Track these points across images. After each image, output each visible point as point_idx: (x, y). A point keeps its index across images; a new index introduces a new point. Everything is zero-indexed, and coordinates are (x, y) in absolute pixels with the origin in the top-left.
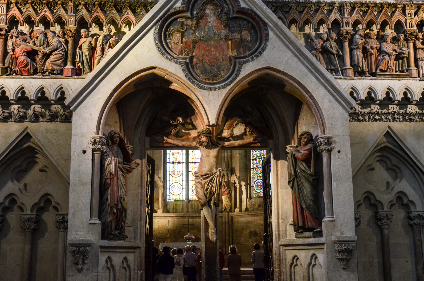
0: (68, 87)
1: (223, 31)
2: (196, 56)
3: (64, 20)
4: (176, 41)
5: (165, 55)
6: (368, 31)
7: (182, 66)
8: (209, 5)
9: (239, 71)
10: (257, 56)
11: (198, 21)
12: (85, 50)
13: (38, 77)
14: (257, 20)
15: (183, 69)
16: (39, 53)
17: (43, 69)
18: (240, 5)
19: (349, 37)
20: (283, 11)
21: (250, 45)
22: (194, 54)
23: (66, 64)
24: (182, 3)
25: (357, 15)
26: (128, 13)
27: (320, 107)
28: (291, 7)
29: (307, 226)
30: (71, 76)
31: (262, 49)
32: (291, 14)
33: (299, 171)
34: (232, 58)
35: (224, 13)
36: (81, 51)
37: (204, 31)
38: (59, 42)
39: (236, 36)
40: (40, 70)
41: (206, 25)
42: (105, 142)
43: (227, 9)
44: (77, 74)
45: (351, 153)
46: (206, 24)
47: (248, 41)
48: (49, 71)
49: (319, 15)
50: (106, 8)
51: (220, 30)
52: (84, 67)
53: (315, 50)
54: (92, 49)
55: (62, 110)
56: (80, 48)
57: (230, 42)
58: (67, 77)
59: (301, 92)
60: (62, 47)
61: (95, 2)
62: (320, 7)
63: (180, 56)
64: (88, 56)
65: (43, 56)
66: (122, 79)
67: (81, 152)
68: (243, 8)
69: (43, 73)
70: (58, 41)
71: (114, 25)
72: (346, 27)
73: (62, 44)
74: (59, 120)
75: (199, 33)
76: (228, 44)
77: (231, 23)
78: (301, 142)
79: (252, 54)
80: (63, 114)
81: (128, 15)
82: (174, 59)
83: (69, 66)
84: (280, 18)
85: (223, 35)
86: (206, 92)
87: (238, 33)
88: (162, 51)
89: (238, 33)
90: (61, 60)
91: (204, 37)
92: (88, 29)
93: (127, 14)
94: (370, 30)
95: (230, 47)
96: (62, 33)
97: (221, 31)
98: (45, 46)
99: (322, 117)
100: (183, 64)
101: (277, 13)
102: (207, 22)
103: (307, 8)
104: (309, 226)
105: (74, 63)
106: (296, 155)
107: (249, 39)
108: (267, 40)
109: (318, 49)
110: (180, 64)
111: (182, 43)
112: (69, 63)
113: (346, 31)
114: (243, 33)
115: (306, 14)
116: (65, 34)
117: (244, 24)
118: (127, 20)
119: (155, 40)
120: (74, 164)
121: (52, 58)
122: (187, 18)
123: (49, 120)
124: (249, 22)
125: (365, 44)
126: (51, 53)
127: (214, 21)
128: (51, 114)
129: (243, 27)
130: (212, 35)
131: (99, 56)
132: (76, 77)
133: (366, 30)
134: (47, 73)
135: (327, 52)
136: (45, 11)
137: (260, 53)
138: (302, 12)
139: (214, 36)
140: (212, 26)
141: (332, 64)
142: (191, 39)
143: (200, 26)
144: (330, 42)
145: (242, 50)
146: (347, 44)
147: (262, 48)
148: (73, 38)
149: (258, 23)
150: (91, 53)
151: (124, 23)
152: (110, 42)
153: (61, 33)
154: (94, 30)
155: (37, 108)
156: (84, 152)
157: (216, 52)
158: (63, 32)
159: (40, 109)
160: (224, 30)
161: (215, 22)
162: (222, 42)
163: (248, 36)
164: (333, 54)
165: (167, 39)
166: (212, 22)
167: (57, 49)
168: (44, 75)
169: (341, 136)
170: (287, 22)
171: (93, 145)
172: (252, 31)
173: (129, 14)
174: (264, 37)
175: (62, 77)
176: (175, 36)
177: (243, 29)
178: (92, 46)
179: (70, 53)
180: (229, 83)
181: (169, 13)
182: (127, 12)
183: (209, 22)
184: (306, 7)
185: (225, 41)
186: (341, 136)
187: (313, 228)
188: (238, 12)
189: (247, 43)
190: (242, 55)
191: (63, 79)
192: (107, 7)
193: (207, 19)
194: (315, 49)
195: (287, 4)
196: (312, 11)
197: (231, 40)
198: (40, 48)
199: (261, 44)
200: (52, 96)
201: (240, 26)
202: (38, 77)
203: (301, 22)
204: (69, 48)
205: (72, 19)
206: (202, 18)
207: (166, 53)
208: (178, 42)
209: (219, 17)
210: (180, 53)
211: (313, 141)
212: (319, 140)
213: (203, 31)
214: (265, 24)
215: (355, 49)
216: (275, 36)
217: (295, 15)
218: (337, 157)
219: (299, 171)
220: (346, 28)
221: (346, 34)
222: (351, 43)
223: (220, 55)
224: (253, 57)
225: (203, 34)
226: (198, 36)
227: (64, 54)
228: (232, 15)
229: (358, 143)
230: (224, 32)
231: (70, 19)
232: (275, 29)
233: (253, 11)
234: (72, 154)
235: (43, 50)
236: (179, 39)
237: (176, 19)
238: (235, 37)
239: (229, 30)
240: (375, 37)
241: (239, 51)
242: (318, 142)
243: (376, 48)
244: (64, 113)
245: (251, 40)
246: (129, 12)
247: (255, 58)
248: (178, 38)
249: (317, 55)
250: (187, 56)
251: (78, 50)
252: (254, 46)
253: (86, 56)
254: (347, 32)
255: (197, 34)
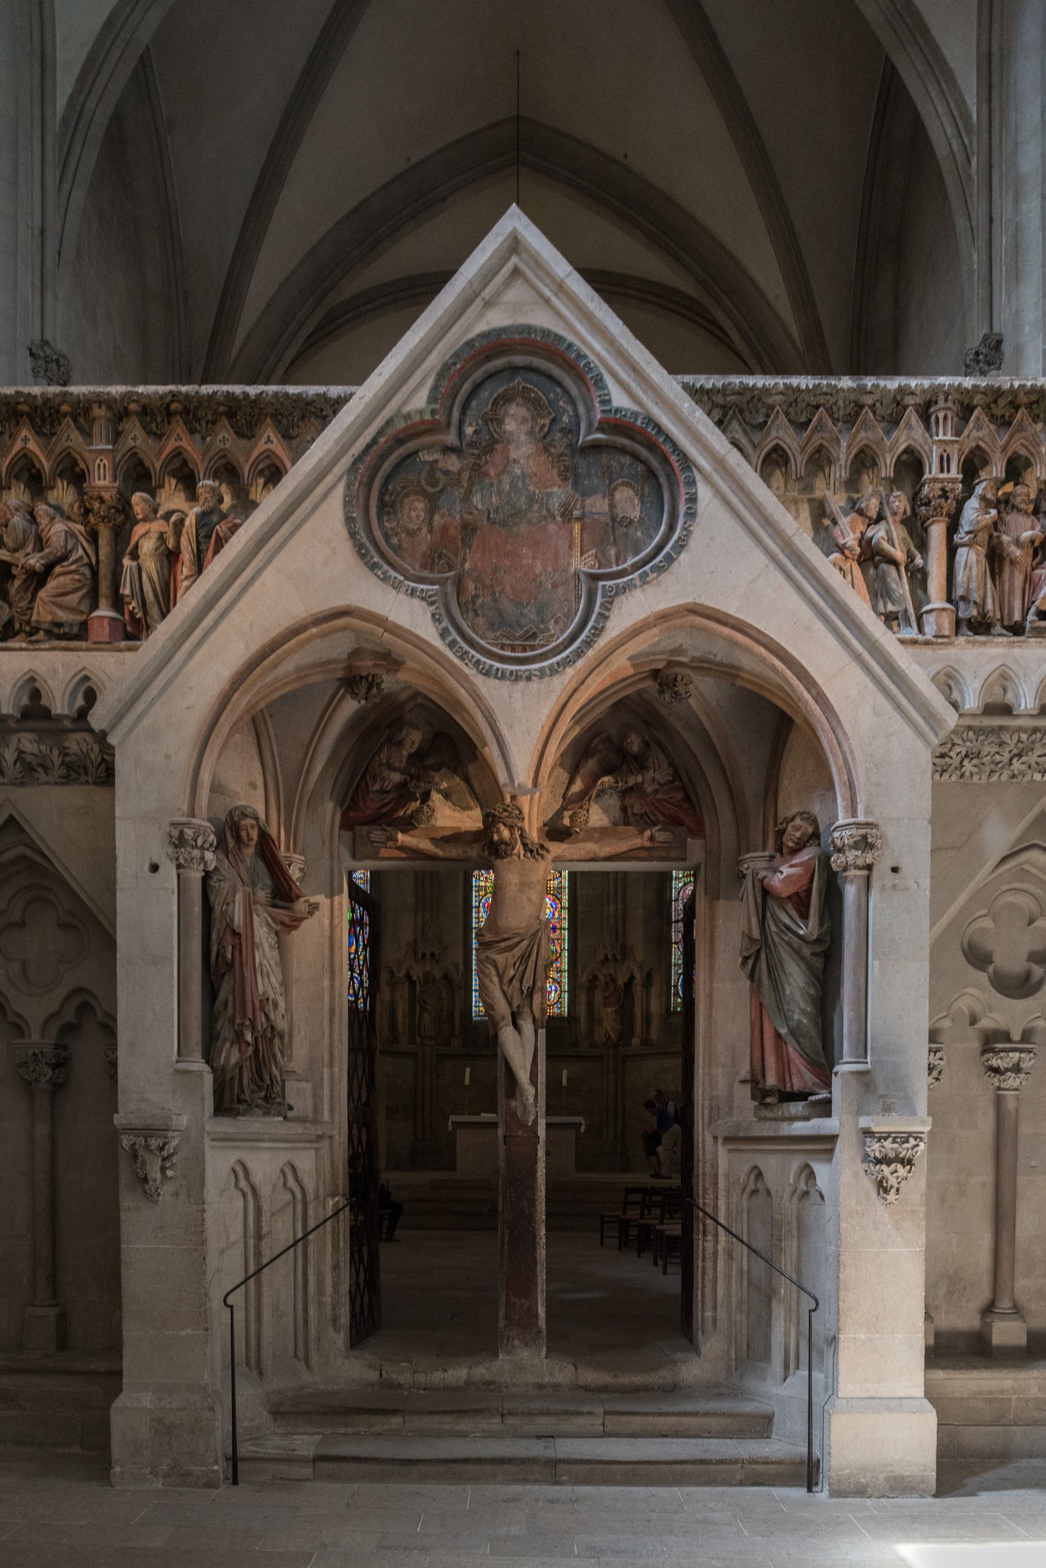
0: (102, 676)
1: (555, 489)
2: (475, 574)
3: (82, 466)
4: (411, 526)
5: (380, 568)
6: (1009, 487)
7: (432, 604)
8: (514, 406)
9: (603, 617)
10: (660, 569)
11: (479, 457)
12: (150, 566)
13: (17, 645)
14: (662, 451)
15: (433, 615)
16: (14, 571)
17: (29, 623)
18: (609, 401)
19: (950, 505)
20: (747, 423)
21: (639, 534)
22: (467, 566)
23: (95, 606)
24: (429, 398)
25: (980, 434)
26: (269, 437)
27: (845, 733)
28: (772, 408)
29: (788, 1085)
30: (108, 643)
31: (673, 547)
32: (768, 433)
33: (774, 928)
34: (582, 577)
35: (561, 430)
36: (134, 564)
37: (498, 490)
38: (70, 534)
39: (598, 504)
40: (21, 625)
41: (503, 471)
42: (212, 838)
43: (569, 415)
44: (128, 637)
45: (932, 877)
46: (506, 467)
47: (631, 522)
48: (46, 626)
49: (858, 432)
50: (204, 423)
51: (547, 487)
52: (145, 613)
53: (843, 553)
54: (170, 557)
55: (96, 748)
56: (135, 556)
57: (577, 527)
58: (97, 646)
59: (791, 685)
60: (81, 552)
61: (168, 405)
62: (862, 407)
63: (426, 574)
64: (156, 579)
65: (25, 581)
66: (255, 647)
67: (147, 867)
68: (618, 410)
69: (30, 634)
70: (66, 532)
71: (230, 484)
72: (942, 471)
73: (78, 540)
74: (90, 780)
75: (483, 496)
76: (571, 532)
77: (583, 465)
78: (782, 843)
79: (645, 562)
80: (99, 760)
81: (269, 446)
82: (406, 582)
83: (104, 611)
84: (735, 444)
85: (555, 504)
86: (505, 686)
87: (604, 497)
88: (372, 557)
89: (604, 497)
90: (80, 594)
91: (497, 510)
92: (153, 493)
93: (266, 443)
94: (1016, 485)
95: (578, 541)
96: (80, 507)
97: (549, 490)
98: (29, 550)
99: (851, 764)
100: (433, 599)
101: (726, 426)
102: (507, 462)
103: (822, 409)
104: (795, 1088)
105: (118, 602)
106: (765, 881)
107: (635, 513)
108: (691, 514)
109: (851, 550)
110: (423, 599)
111: (431, 531)
112: (103, 602)
113: (940, 485)
114: (618, 496)
115: (815, 430)
116: (87, 512)
117: (622, 467)
118: (267, 462)
119: (349, 520)
120: (126, 904)
121: (52, 584)
122: (447, 449)
123: (63, 777)
124: (637, 458)
125: (996, 529)
126: (49, 568)
127: (528, 458)
128: (67, 759)
129: (618, 478)
130: (522, 503)
131: (186, 578)
132: (123, 644)
133: (1004, 483)
134: (42, 633)
135: (877, 558)
136: (26, 440)
137: (670, 559)
138: (805, 425)
139: (530, 506)
140: (522, 472)
141: (890, 598)
142: (458, 518)
143: (486, 475)
144: (888, 523)
145: (613, 552)
146: (937, 532)
147: (677, 541)
148: (109, 521)
149: (665, 460)
150: (166, 571)
151: (261, 473)
152: (218, 534)
153: (75, 509)
154: (172, 498)
155: (29, 743)
156: (154, 868)
157: (534, 558)
158: (82, 504)
159: (35, 745)
160: (560, 486)
161: (531, 462)
162: (552, 527)
163: (633, 504)
164: (895, 563)
165: (385, 518)
166: (522, 461)
167: (64, 558)
168: (33, 638)
169: (906, 821)
170: (758, 457)
171: (176, 846)
172: (646, 490)
173: (272, 442)
174: (682, 508)
175: (84, 644)
176: (410, 509)
177: (620, 481)
178: (167, 548)
179: (104, 570)
180: (571, 657)
181: (390, 432)
182: (265, 436)
183: (515, 461)
184: (817, 407)
185: (563, 522)
186: (906, 821)
187: (807, 1090)
188: (601, 429)
189: (631, 532)
190: (615, 569)
191: (87, 650)
192: (207, 422)
193: (506, 451)
194: (841, 549)
195: (759, 399)
196: (838, 420)
197: (578, 519)
198: (17, 555)
199: (671, 528)
200: (59, 705)
201: (609, 475)
202: (17, 645)
203: (799, 458)
204: (101, 553)
205: (105, 461)
206: (489, 448)
207: (382, 562)
208: (420, 529)
209: (544, 442)
210: (426, 563)
211: (819, 839)
212: (836, 834)
213: (494, 489)
214: (687, 463)
215: (962, 545)
216: (717, 503)
217: (781, 433)
218: (889, 885)
219: (774, 928)
220: (941, 476)
221: (940, 497)
222: (953, 528)
223: (545, 569)
224: (645, 573)
225: (494, 500)
226: (480, 507)
227: (87, 571)
228: (584, 438)
229: (951, 848)
230: (559, 493)
231: (98, 461)
232: (716, 478)
233: (650, 420)
234: (119, 875)
235: (23, 561)
236: (421, 519)
237: (415, 453)
238: (594, 510)
239: (576, 484)
240: (1031, 507)
241: (603, 553)
242: (833, 841)
243: (1032, 542)
244: (103, 759)
245: (641, 519)
246: (272, 435)
247: (652, 576)
248: (418, 516)
249: (846, 567)
250: (447, 575)
251: (127, 562)
252: (652, 538)
253: (150, 579)
254: (943, 489)
255: (477, 499)
